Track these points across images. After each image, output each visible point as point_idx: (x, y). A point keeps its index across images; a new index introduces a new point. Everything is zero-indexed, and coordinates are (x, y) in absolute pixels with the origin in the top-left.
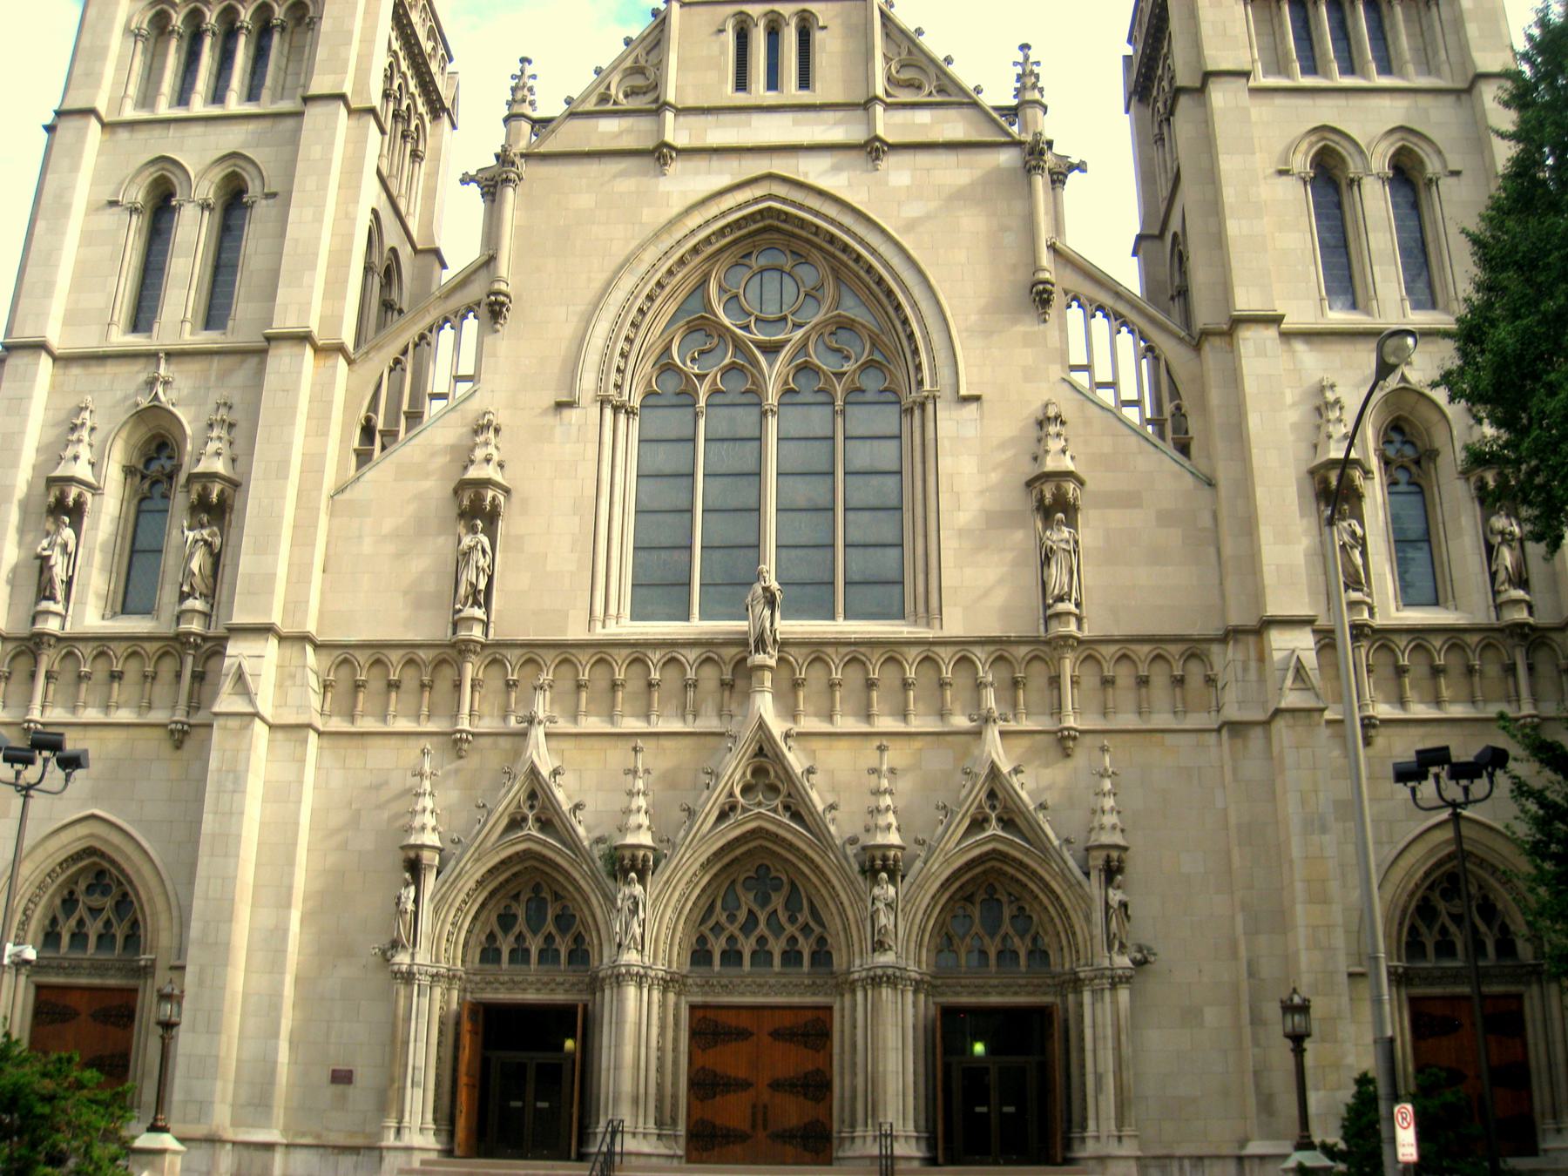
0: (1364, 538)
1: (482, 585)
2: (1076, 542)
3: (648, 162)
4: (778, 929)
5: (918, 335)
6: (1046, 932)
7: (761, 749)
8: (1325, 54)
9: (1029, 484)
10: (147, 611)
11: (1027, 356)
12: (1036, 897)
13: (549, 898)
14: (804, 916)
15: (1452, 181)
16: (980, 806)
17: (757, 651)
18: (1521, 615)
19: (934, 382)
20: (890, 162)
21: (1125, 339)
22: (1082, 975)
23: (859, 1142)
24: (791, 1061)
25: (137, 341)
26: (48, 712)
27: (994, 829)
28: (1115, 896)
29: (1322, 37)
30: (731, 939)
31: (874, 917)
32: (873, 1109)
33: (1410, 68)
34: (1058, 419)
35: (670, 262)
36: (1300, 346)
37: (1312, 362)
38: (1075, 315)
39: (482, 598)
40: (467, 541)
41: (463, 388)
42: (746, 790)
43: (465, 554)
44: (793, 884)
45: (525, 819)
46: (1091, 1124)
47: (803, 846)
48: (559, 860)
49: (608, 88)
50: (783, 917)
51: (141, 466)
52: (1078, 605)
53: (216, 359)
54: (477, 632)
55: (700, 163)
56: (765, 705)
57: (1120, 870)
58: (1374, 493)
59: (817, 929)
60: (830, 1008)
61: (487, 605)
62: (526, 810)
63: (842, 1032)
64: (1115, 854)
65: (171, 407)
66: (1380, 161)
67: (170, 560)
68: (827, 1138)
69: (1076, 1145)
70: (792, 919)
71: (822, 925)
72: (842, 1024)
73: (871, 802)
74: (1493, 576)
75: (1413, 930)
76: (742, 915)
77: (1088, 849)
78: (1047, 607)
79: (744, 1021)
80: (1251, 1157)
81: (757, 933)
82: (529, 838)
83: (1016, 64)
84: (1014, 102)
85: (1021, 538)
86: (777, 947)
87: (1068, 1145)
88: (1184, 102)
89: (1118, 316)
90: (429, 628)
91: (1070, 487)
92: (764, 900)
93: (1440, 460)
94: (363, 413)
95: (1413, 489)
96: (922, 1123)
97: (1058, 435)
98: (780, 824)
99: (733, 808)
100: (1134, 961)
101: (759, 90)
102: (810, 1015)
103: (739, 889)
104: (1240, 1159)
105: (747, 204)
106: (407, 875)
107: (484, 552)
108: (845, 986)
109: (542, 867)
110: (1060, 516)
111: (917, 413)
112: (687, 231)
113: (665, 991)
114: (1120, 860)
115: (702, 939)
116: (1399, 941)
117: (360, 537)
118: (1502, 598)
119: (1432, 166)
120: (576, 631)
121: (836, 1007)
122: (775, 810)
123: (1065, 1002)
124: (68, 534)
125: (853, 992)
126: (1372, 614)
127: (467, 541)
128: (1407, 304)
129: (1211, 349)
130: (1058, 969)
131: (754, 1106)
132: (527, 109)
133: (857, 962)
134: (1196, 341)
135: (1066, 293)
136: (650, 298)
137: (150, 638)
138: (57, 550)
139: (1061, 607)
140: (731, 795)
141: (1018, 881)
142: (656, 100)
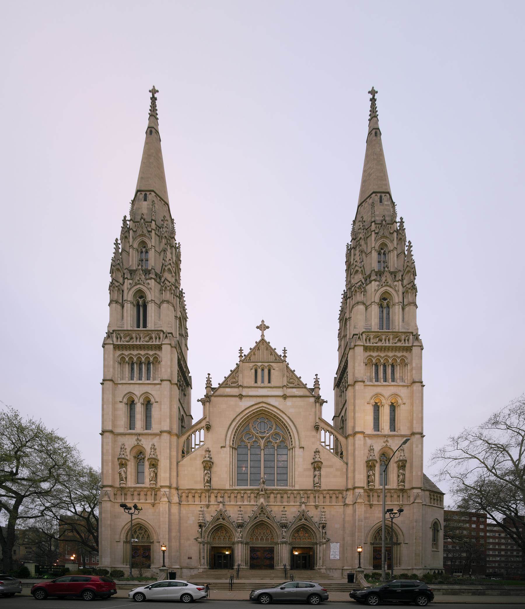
3: (237, 399)
9: (312, 463)
55: (248, 399)
78: (314, 485)
98: (266, 519)
99: (257, 517)
101: (259, 383)
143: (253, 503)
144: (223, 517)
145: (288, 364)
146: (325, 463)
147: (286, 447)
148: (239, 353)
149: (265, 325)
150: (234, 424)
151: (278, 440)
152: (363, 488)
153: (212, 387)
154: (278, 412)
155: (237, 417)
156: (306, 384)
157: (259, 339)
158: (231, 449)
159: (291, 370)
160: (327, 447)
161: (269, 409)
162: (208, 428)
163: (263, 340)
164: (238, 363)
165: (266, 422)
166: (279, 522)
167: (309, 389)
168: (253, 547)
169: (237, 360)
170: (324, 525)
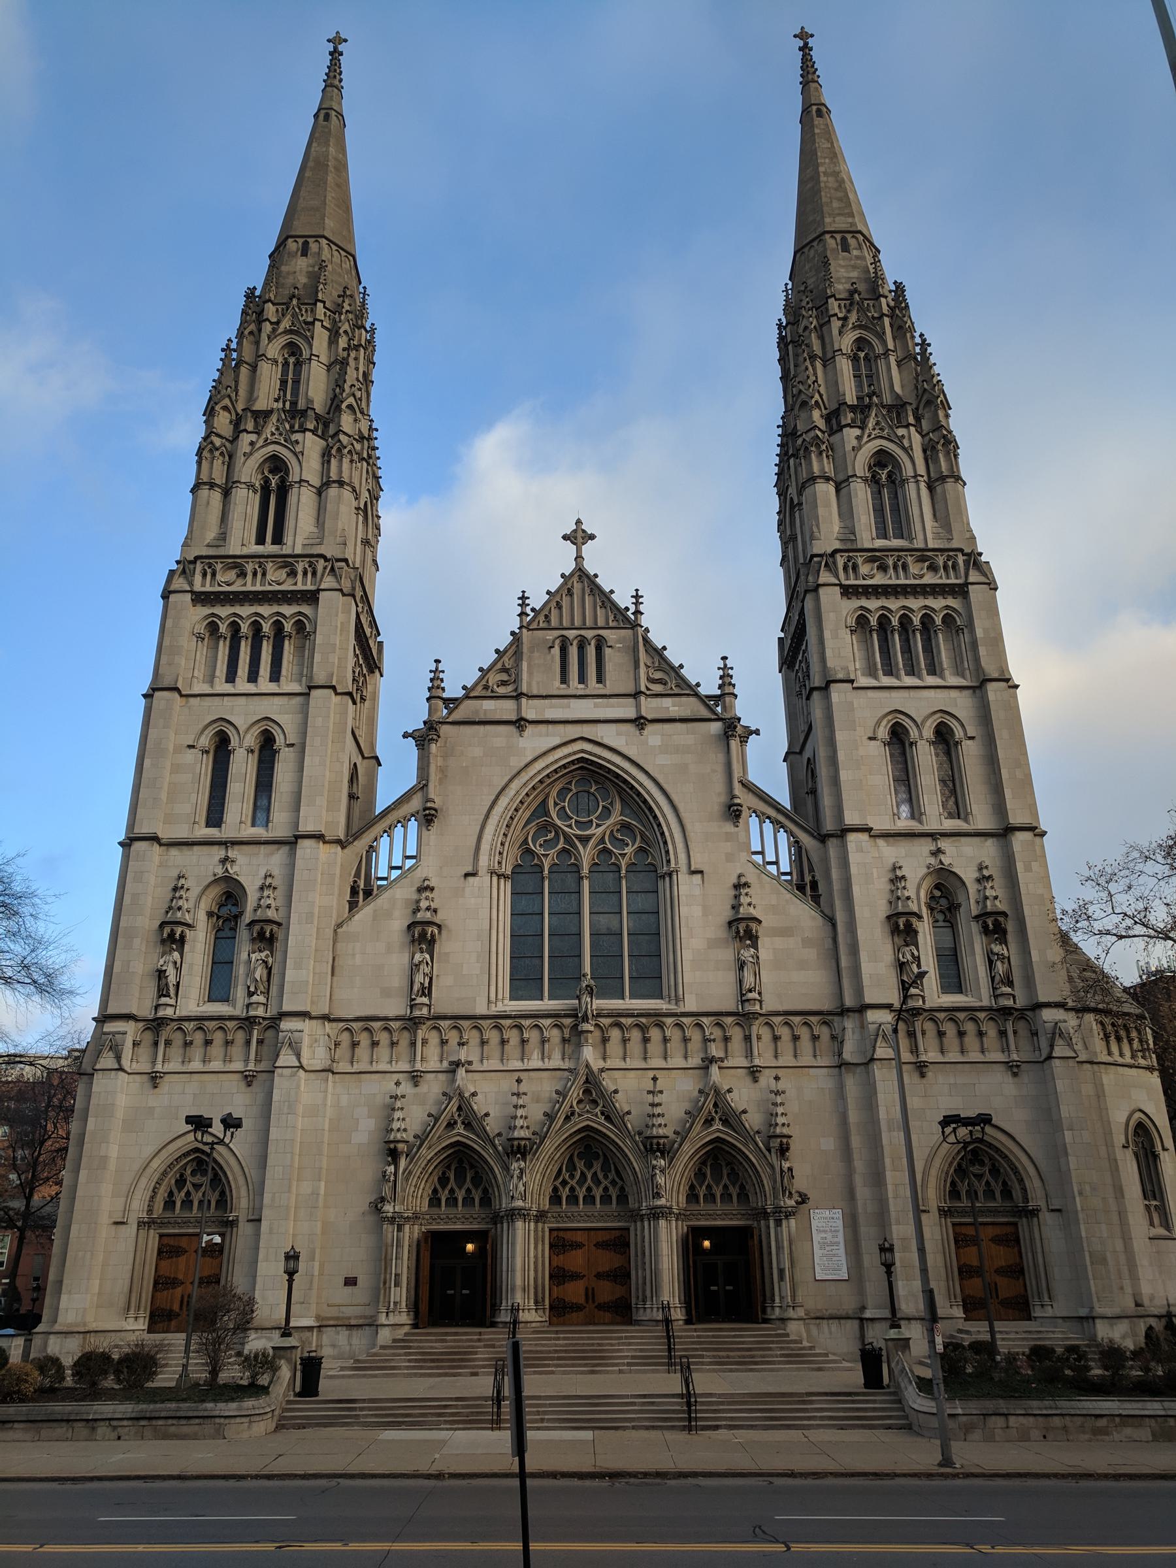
0: (919, 957)
1: (426, 985)
2: (758, 958)
4: (598, 1183)
5: (667, 834)
6: (747, 1183)
7: (587, 1079)
8: (897, 664)
9: (730, 923)
10: (226, 1000)
11: (728, 847)
12: (741, 1163)
13: (467, 1167)
14: (612, 1175)
15: (969, 742)
16: (710, 1112)
17: (583, 1021)
18: (1009, 1003)
19: (677, 863)
20: (650, 728)
21: (782, 836)
22: (769, 1210)
23: (648, 1311)
24: (607, 1261)
25: (213, 832)
26: (166, 1065)
27: (717, 1125)
28: (786, 1165)
29: (896, 654)
30: (572, 1189)
31: (654, 1176)
32: (656, 1289)
33: (947, 673)
34: (746, 885)
35: (527, 789)
36: (881, 842)
37: (889, 852)
38: (754, 821)
39: (427, 991)
40: (418, 957)
41: (409, 863)
42: (580, 1102)
43: (416, 965)
44: (605, 1155)
45: (455, 1123)
46: (777, 1299)
47: (613, 1136)
48: (475, 1146)
49: (487, 682)
50: (600, 1176)
51: (216, 911)
52: (760, 994)
53: (262, 847)
54: (425, 1011)
56: (589, 1054)
57: (788, 1149)
58: (925, 931)
59: (620, 1183)
60: (628, 1229)
61: (430, 995)
62: (456, 1117)
63: (636, 1244)
64: (785, 1140)
65: (236, 877)
66: (928, 732)
67: (241, 971)
68: (629, 1307)
69: (769, 1310)
70: (606, 1177)
71: (622, 1179)
72: (636, 1239)
73: (649, 1110)
74: (993, 979)
75: (953, 1183)
76: (578, 1175)
77: (770, 1137)
78: (742, 995)
79: (579, 1237)
80: (868, 1319)
81: (586, 1185)
82: (459, 1134)
83: (719, 668)
84: (719, 692)
85: (727, 955)
86: (598, 1193)
87: (764, 1311)
88: (816, 695)
89: (778, 822)
90: (396, 1007)
91: (753, 925)
92: (589, 1166)
93: (962, 910)
94: (352, 879)
95: (948, 924)
96: (683, 1298)
97: (747, 894)
99: (573, 1114)
100: (797, 1202)
102: (618, 1233)
103: (576, 1159)
104: (861, 1319)
105: (570, 755)
106: (390, 1159)
107: (427, 963)
108: (636, 1216)
109: (465, 1150)
110: (748, 942)
111: (667, 879)
112: (536, 771)
113: (537, 1222)
114: (788, 1144)
115: (555, 1189)
116: (945, 1191)
117: (354, 955)
118: (998, 992)
119: (959, 733)
120: (481, 1010)
121: (632, 1229)
122: (596, 1115)
123: (759, 1224)
124: (176, 955)
125: (642, 1221)
126: (924, 1002)
127: (418, 957)
128: (943, 817)
129: (832, 844)
130: (755, 1205)
131: (587, 1289)
132: (439, 693)
133: (644, 1204)
134: (823, 838)
135: (749, 809)
136: (516, 810)
137: (231, 1018)
138: (171, 966)
139: (751, 995)
140: (571, 1107)
141: (730, 1153)
142: (516, 690)
143: (556, 1062)
144: (467, 1116)
145: (647, 630)
146: (768, 921)
147: (652, 868)
148: (519, 605)
149: (584, 531)
150: (503, 802)
151: (627, 845)
152: (888, 1007)
153: (445, 695)
154: (626, 765)
155: (511, 780)
156: (698, 685)
157: (569, 567)
158: (495, 879)
159: (655, 649)
160: (769, 867)
161: (600, 757)
162: (428, 817)
163: (580, 572)
164: (517, 631)
165: (592, 790)
166: (640, 1133)
167: (707, 697)
168: (558, 1229)
169: (515, 625)
170: (785, 1140)
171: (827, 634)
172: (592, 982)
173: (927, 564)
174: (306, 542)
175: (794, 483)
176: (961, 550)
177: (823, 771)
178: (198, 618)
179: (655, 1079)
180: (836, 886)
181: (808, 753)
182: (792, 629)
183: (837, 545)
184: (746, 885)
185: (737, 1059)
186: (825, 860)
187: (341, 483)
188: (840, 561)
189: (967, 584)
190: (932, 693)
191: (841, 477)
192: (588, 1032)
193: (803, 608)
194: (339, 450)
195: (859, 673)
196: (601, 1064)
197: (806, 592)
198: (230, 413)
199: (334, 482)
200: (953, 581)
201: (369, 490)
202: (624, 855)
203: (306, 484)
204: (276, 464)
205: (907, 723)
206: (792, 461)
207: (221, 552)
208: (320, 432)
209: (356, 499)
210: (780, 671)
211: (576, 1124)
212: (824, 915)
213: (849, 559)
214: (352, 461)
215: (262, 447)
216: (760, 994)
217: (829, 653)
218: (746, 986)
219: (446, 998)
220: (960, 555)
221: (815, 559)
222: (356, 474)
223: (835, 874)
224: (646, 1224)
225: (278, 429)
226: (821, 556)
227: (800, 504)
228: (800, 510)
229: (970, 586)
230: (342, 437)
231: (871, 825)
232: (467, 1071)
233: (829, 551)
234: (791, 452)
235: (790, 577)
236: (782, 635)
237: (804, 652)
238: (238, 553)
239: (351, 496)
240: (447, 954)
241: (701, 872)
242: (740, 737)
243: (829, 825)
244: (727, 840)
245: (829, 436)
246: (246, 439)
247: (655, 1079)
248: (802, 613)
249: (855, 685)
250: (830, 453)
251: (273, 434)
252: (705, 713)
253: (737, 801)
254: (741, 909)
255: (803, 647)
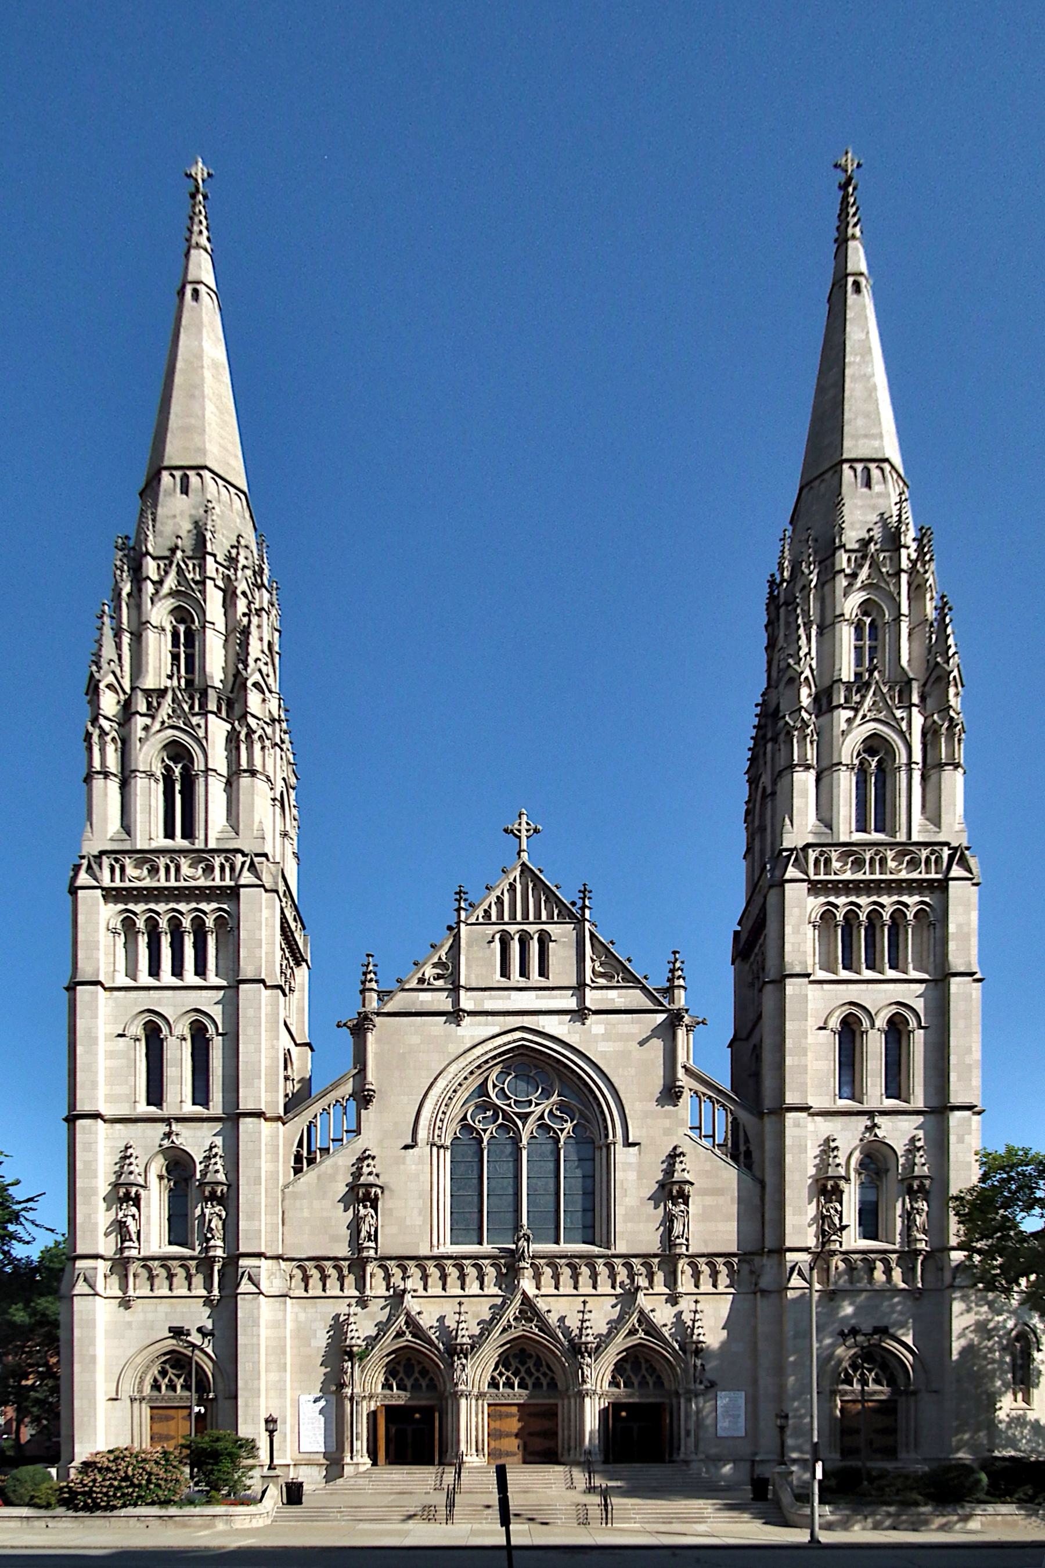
1: (373, 1233)
4: (530, 1374)
11: (667, 1123)
14: (545, 1369)
19: (614, 1136)
34: (682, 1154)
36: (818, 1119)
37: (824, 1127)
42: (516, 1319)
50: (533, 1370)
52: (687, 1240)
54: (372, 1253)
60: (556, 1405)
61: (376, 1240)
66: (881, 1022)
68: (556, 1454)
91: (687, 1187)
92: (523, 1363)
99: (510, 1326)
115: (493, 1378)
120: (424, 1251)
134: (761, 1115)
135: (691, 1090)
140: (509, 1321)
171: (788, 929)
172: (529, 1232)
173: (907, 858)
174: (218, 836)
175: (769, 771)
176: (947, 844)
177: (767, 1056)
178: (111, 913)
179: (584, 1302)
180: (769, 1154)
181: (754, 1040)
182: (750, 923)
183: (811, 839)
184: (682, 1154)
185: (660, 1287)
186: (761, 1134)
187: (253, 773)
188: (812, 855)
189: (947, 879)
190: (891, 986)
191: (825, 764)
192: (524, 1268)
193: (765, 902)
194: (248, 735)
195: (817, 966)
196: (537, 1292)
197: (771, 887)
198: (117, 693)
199: (245, 771)
200: (933, 876)
201: (284, 779)
202: (562, 1130)
203: (213, 773)
204: (176, 752)
205: (860, 1013)
206: (769, 746)
207: (127, 846)
208: (224, 714)
209: (272, 789)
210: (733, 963)
211: (512, 1334)
212: (754, 1178)
213: (822, 854)
214: (263, 748)
215: (159, 731)
216: (687, 1240)
217: (788, 947)
218: (675, 1233)
219: (390, 1242)
220: (946, 849)
221: (785, 854)
222: (269, 762)
223: (769, 1145)
224: (572, 1401)
225: (174, 711)
226: (791, 850)
227: (774, 793)
228: (773, 800)
229: (951, 883)
230: (251, 721)
231: (810, 1104)
232: (413, 1297)
233: (800, 845)
234: (769, 735)
235: (753, 871)
236: (739, 928)
237: (761, 946)
238: (146, 847)
239: (266, 786)
240: (391, 1210)
241: (639, 1144)
242: (687, 1026)
243: (768, 1103)
244: (666, 1117)
245: (817, 717)
246: (140, 722)
247: (584, 1302)
248: (763, 909)
249: (812, 978)
250: (815, 737)
251: (169, 717)
252: (651, 1006)
253: (679, 1083)
254: (676, 1175)
255: (761, 941)
